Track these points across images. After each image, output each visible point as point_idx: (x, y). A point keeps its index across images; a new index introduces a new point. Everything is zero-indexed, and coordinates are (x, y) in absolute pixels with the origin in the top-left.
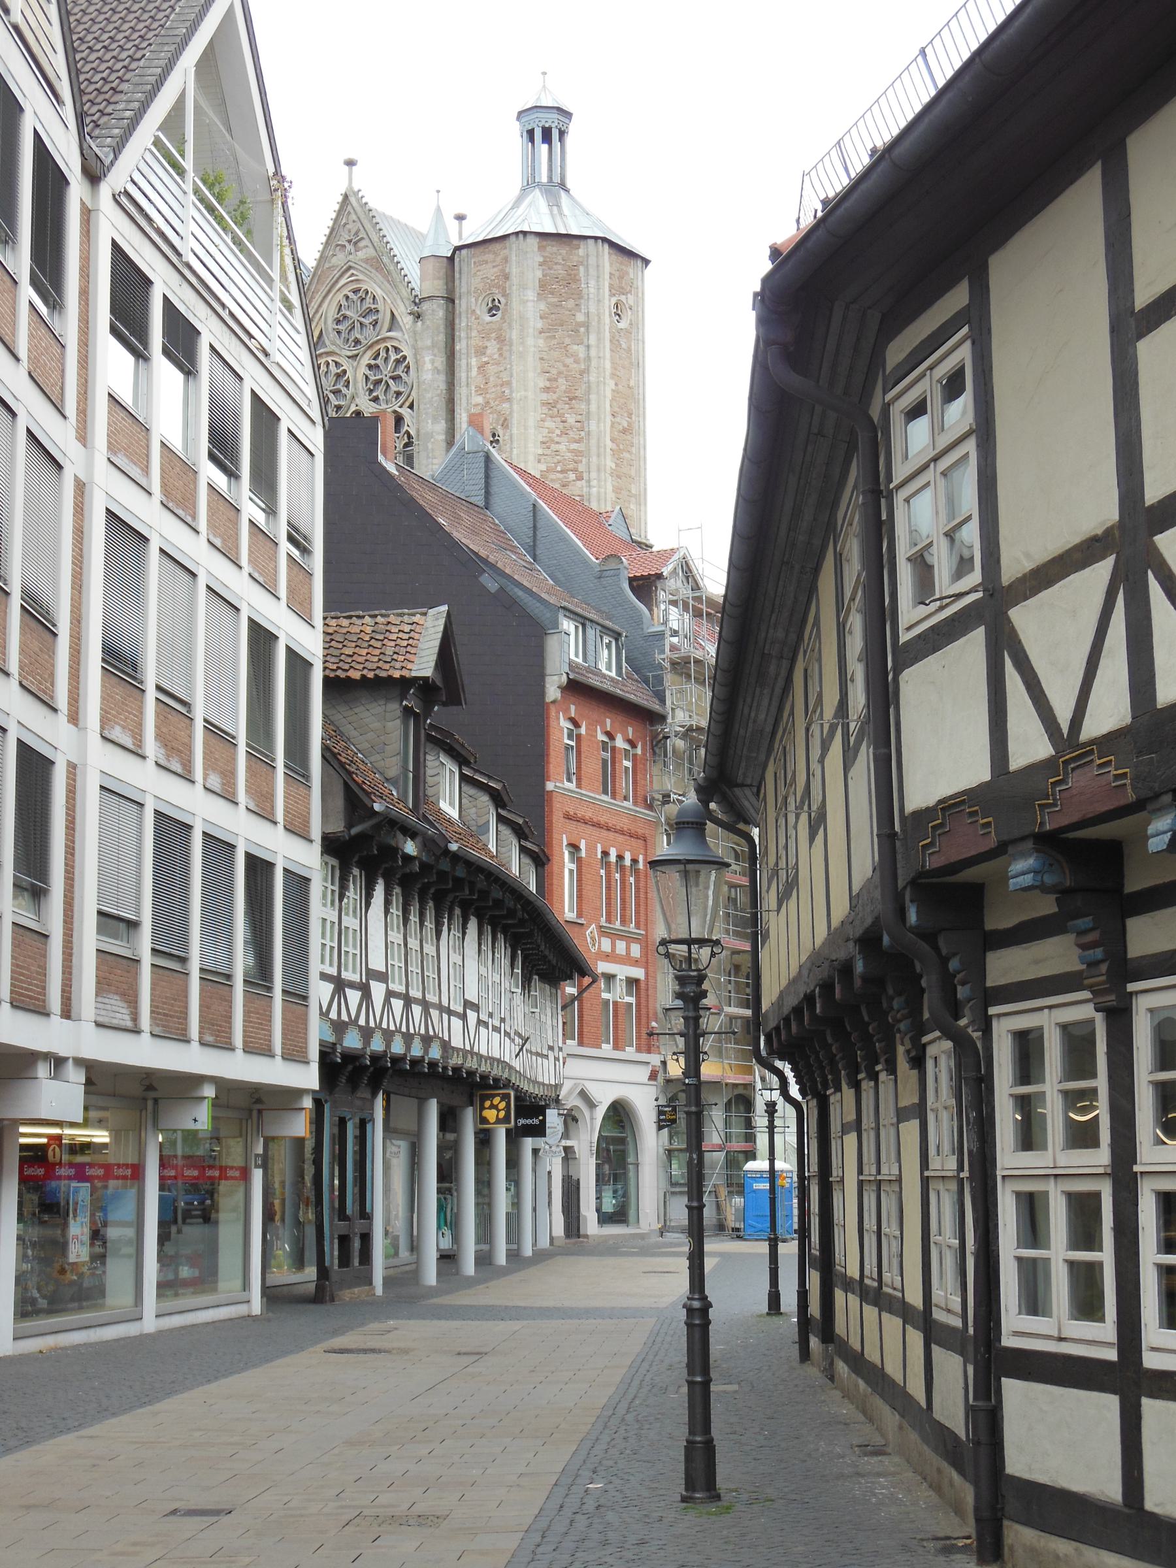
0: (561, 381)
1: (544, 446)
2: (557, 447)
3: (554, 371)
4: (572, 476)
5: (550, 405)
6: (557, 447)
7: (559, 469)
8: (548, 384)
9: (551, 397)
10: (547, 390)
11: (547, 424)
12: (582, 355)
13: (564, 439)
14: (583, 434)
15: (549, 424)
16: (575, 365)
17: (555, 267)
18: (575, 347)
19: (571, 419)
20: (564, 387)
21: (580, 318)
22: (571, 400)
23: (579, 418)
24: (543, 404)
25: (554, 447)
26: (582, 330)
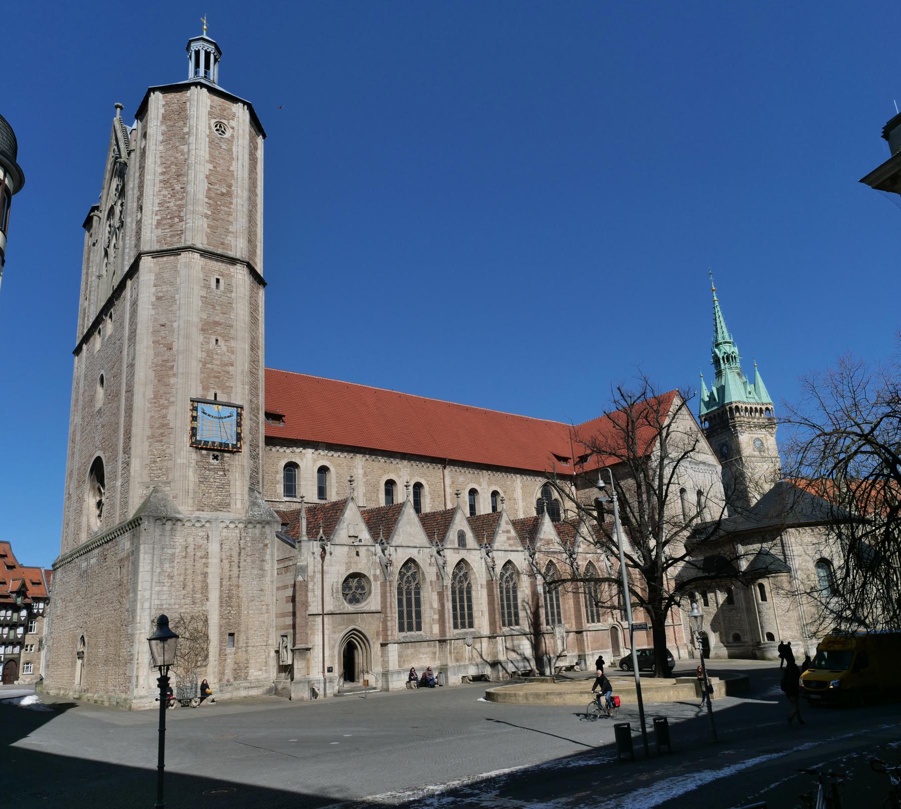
0: (173, 167)
1: (160, 205)
2: (168, 205)
3: (169, 162)
4: (177, 220)
5: (164, 182)
6: (168, 205)
7: (169, 217)
8: (164, 170)
9: (166, 177)
10: (163, 173)
11: (162, 193)
12: (186, 150)
13: (173, 200)
14: (184, 194)
15: (165, 192)
16: (182, 157)
17: (172, 105)
18: (182, 147)
19: (178, 187)
20: (174, 170)
21: (186, 130)
22: (178, 176)
23: (183, 186)
24: (161, 182)
25: (166, 205)
26: (187, 136)
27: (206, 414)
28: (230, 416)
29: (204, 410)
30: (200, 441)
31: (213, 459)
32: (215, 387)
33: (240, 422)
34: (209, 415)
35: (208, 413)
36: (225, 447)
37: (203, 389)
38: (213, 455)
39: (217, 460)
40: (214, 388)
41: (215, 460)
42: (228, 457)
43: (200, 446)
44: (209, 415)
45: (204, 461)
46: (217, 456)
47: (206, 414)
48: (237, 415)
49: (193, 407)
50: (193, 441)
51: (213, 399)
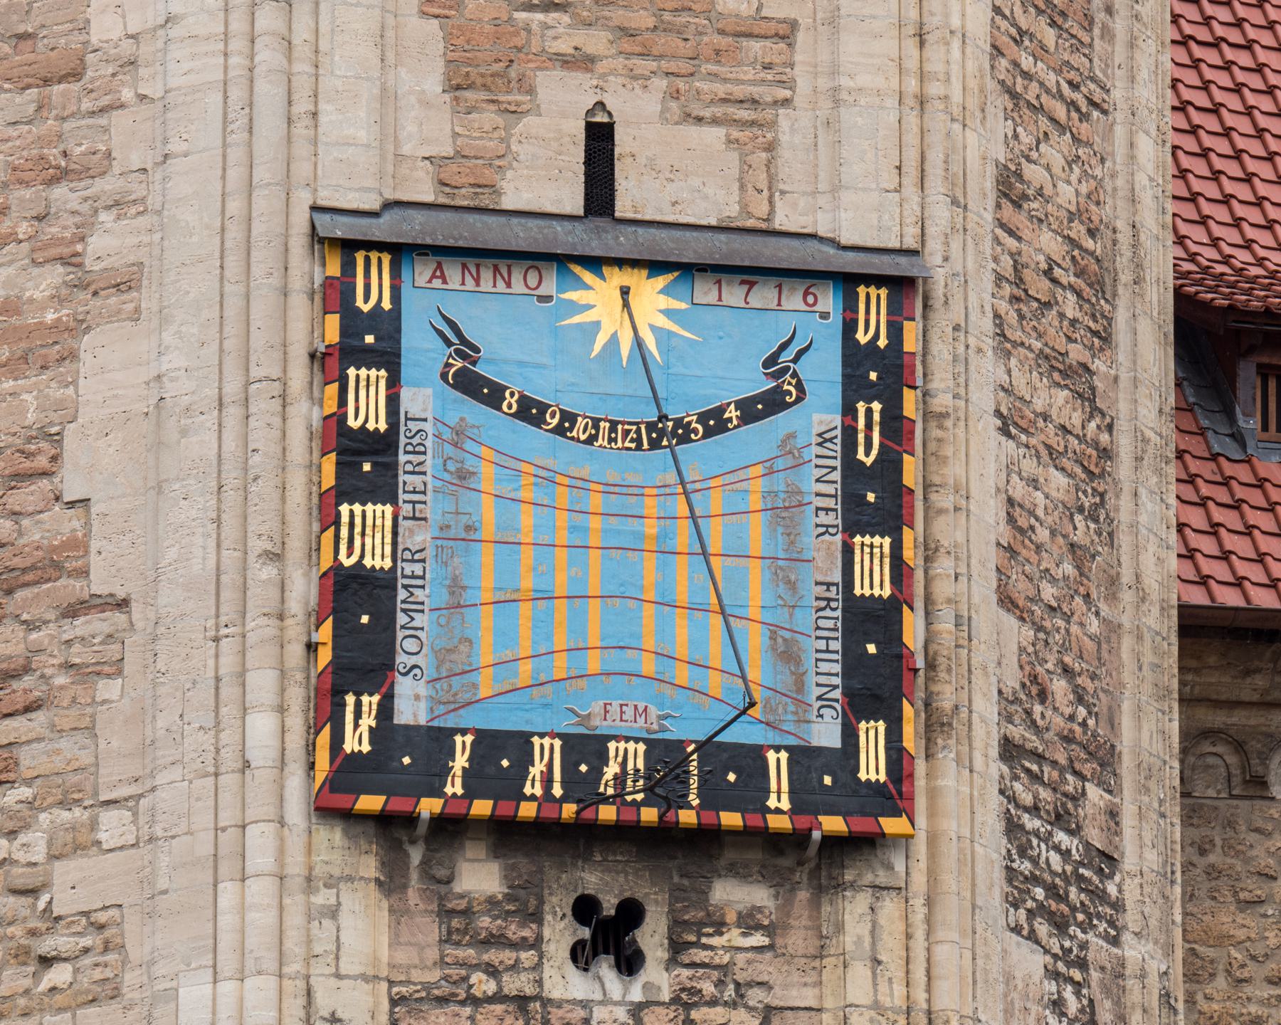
27: (492, 395)
28: (773, 403)
29: (467, 350)
30: (440, 740)
31: (581, 956)
32: (596, 42)
33: (890, 464)
34: (531, 412)
35: (516, 384)
36: (714, 797)
37: (455, 87)
38: (585, 909)
39: (630, 964)
40: (581, 62)
41: (606, 969)
42: (749, 922)
43: (429, 807)
44: (531, 412)
45: (483, 985)
46: (631, 913)
47: (492, 395)
48: (854, 388)
49: (353, 322)
50: (357, 741)
51: (571, 198)
